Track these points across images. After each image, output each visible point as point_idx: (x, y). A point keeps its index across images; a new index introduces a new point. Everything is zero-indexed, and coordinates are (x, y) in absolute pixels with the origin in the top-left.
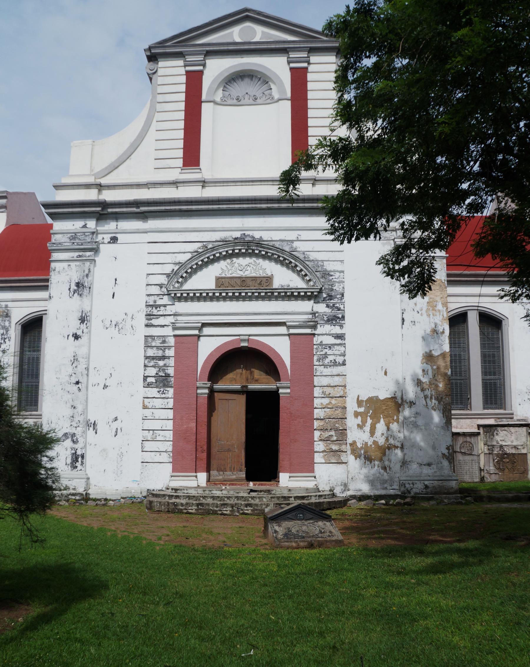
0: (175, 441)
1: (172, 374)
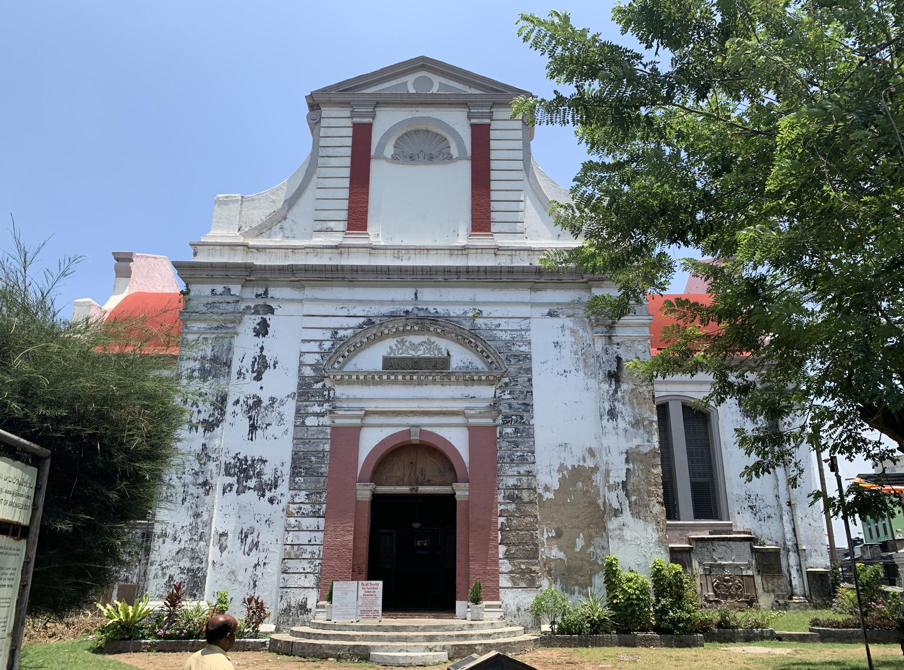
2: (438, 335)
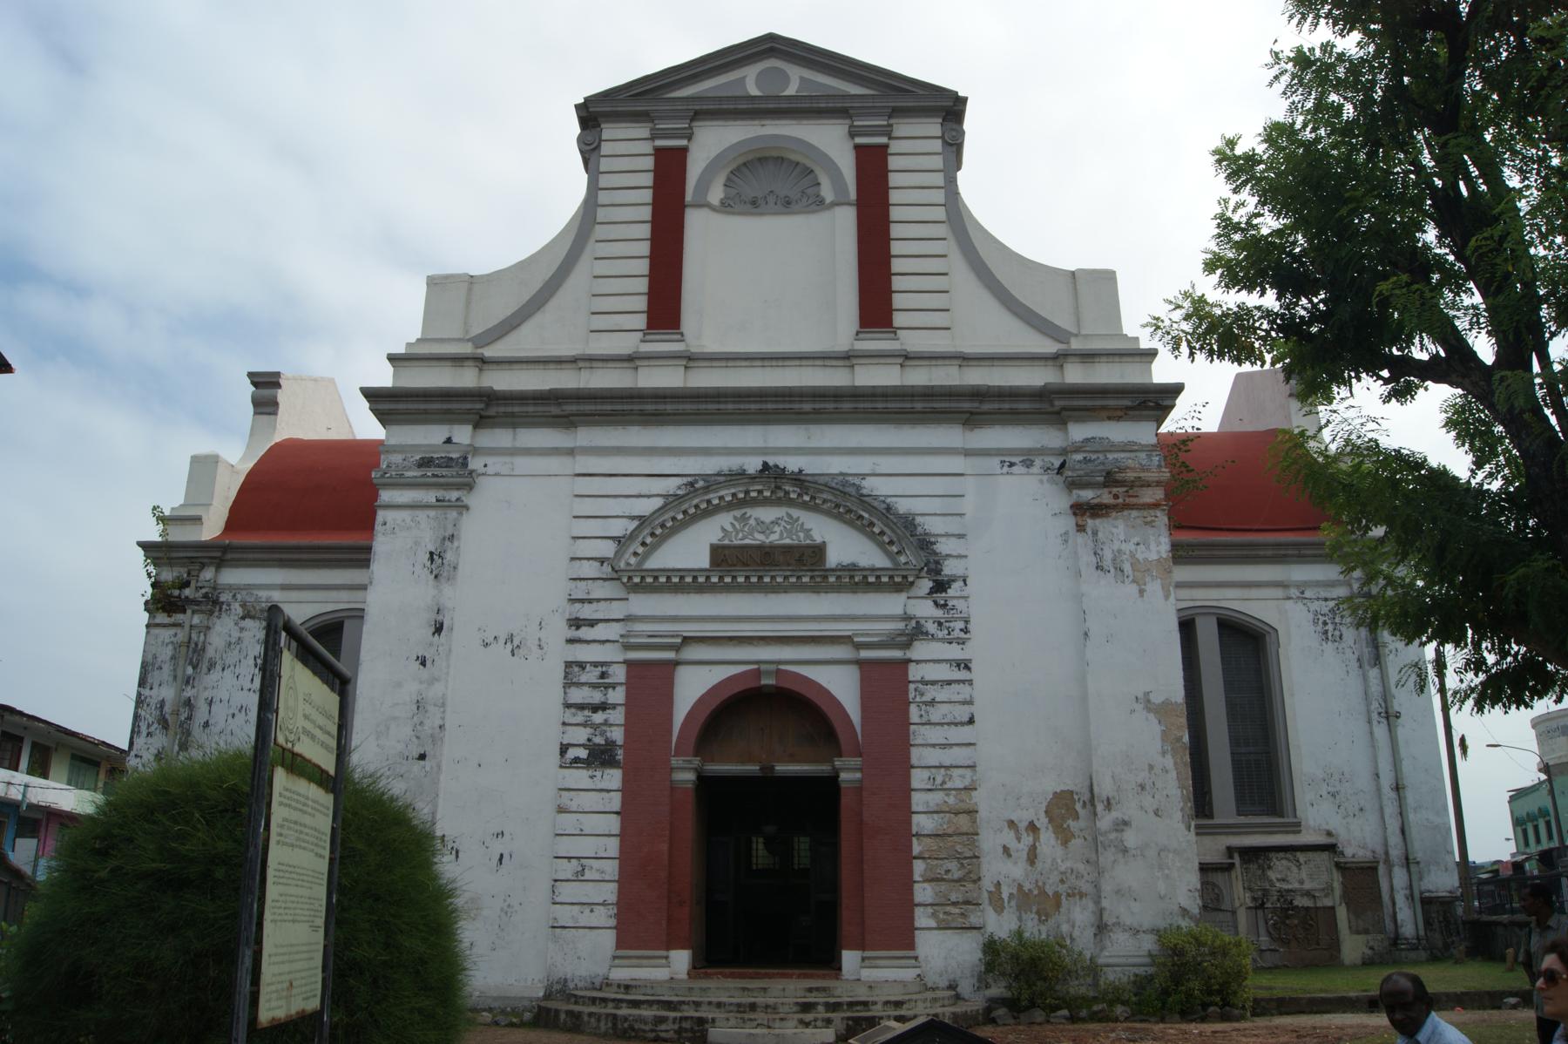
0: (624, 881)
1: (620, 742)
2: (805, 506)
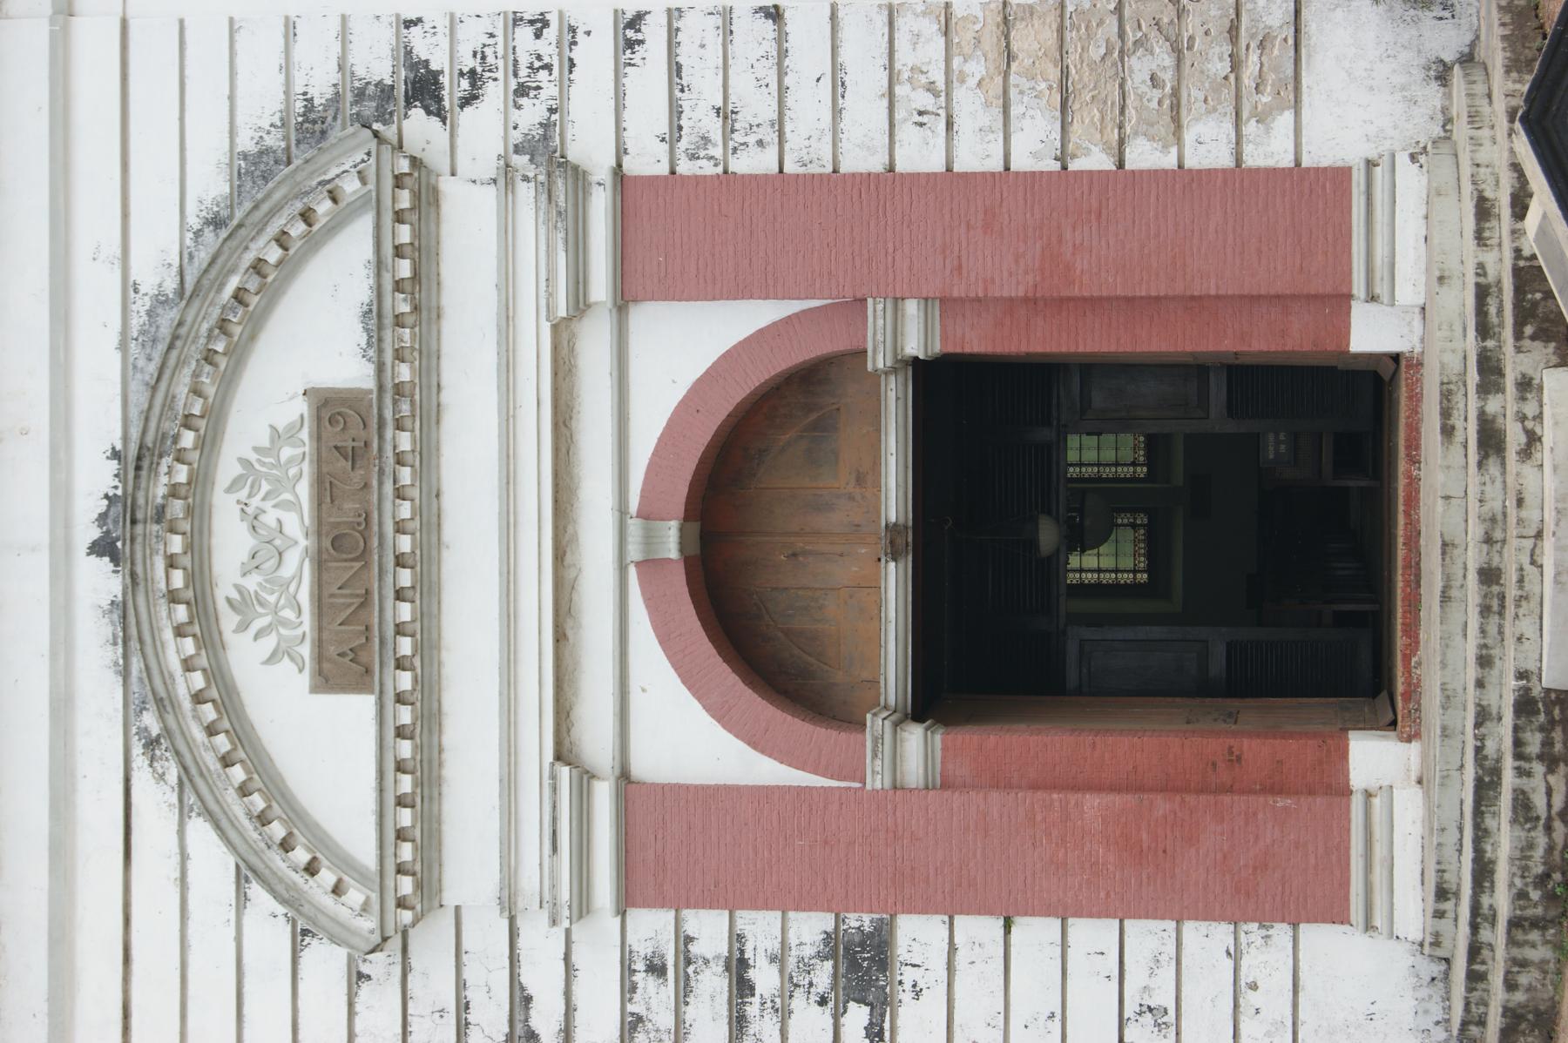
0: (1180, 906)
1: (826, 921)
2: (209, 444)
